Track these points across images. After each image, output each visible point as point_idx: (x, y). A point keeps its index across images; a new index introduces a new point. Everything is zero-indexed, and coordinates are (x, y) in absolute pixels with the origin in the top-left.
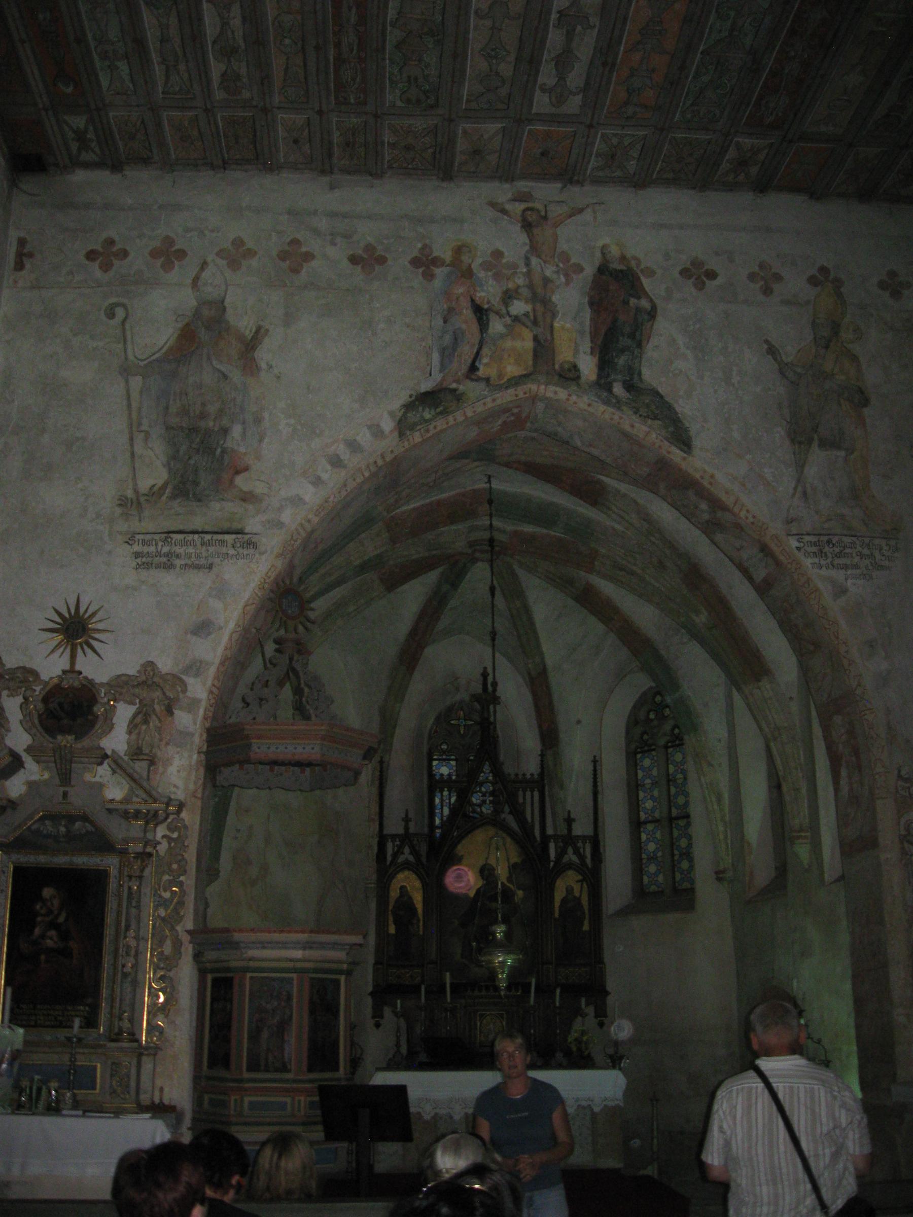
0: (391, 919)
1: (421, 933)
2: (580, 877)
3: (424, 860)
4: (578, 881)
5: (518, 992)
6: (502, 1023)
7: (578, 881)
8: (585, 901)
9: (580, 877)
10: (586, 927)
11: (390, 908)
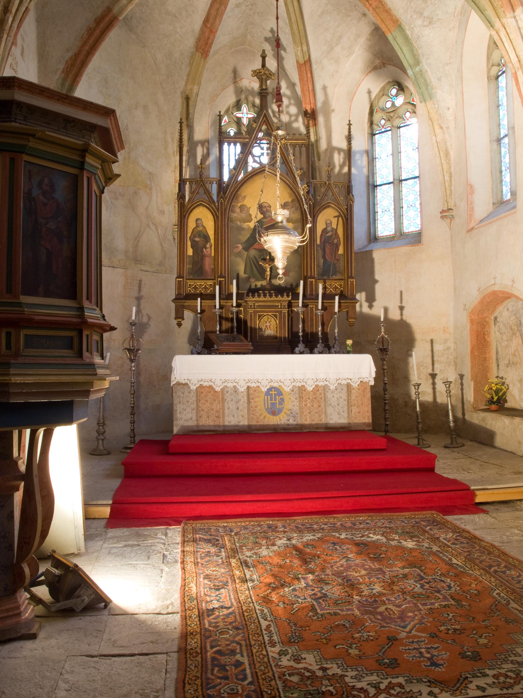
0: (189, 243)
1: (213, 255)
2: (337, 214)
3: (215, 197)
4: (335, 217)
5: (288, 297)
6: (276, 321)
7: (335, 217)
8: (340, 232)
9: (337, 214)
10: (341, 251)
11: (189, 235)
